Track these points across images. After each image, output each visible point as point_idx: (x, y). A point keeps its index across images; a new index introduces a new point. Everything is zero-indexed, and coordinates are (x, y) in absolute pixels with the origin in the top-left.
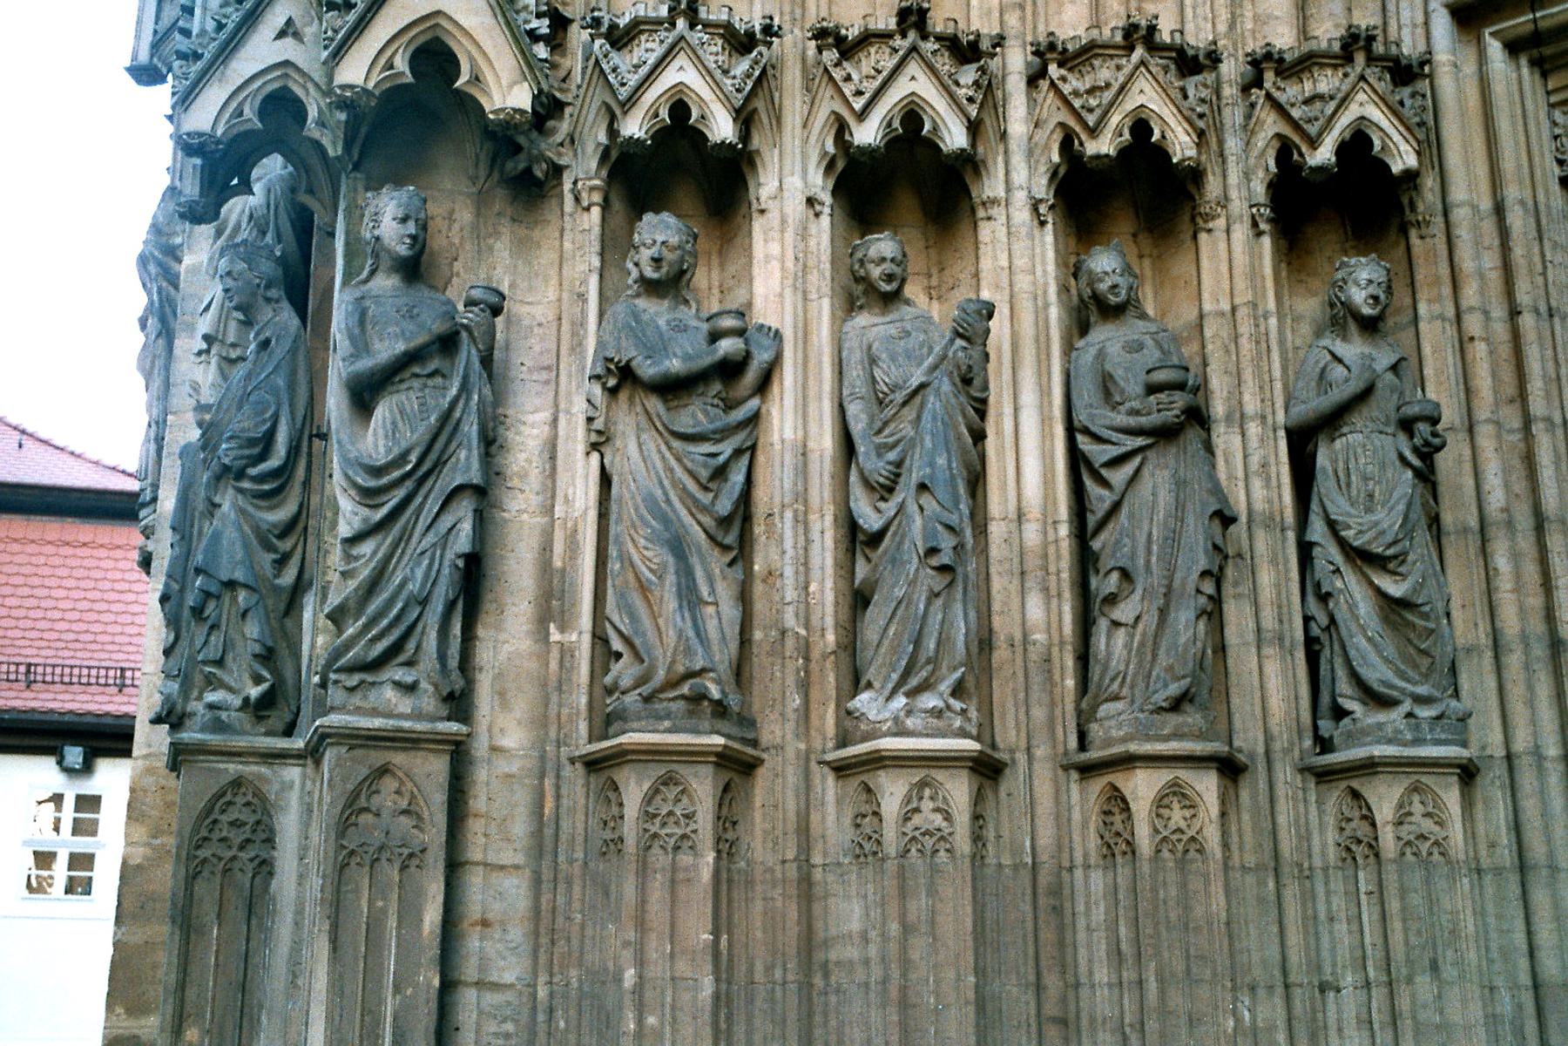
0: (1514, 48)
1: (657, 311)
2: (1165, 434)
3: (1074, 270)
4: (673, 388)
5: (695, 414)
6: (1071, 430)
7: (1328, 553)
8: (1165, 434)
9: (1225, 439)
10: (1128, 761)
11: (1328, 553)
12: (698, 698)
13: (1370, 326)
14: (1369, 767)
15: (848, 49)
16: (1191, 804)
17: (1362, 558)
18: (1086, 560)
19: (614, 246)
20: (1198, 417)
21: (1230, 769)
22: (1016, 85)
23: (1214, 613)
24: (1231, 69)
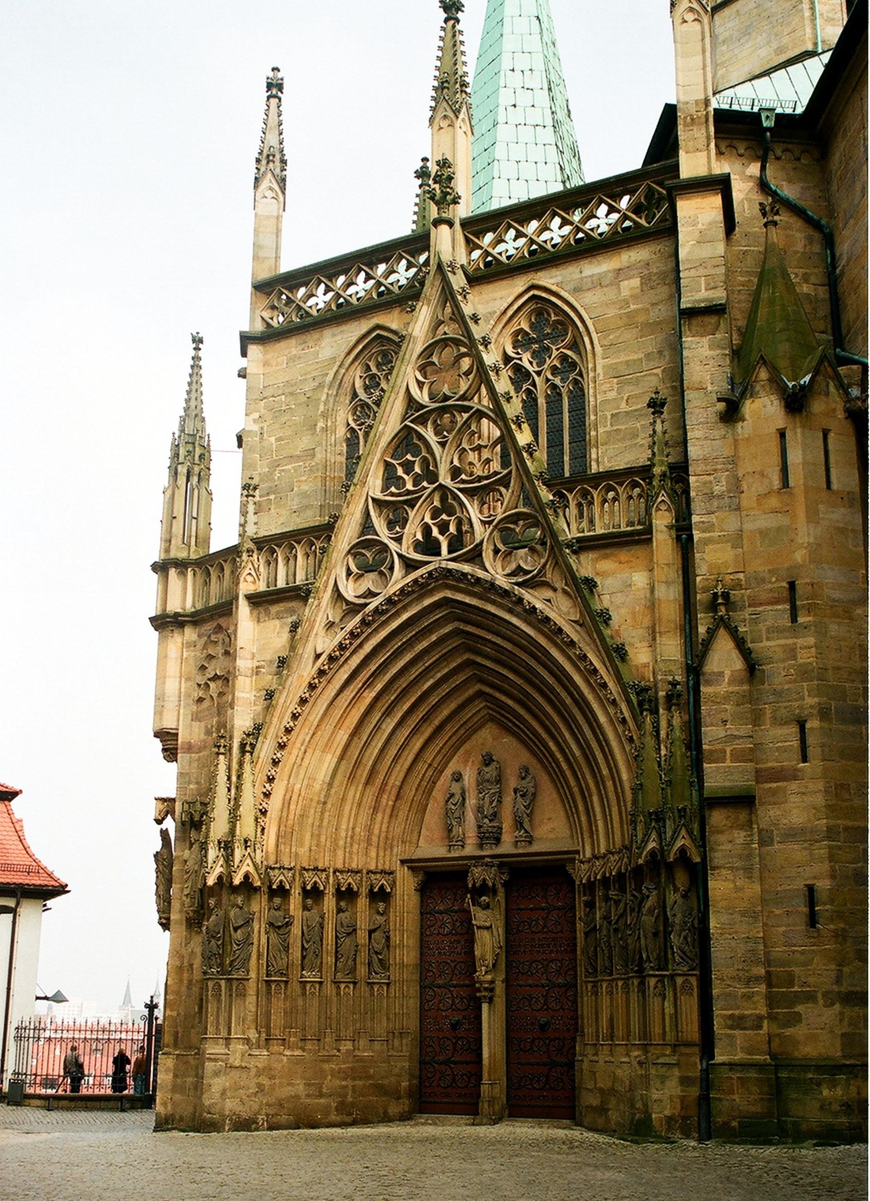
0: (409, 868)
1: (277, 913)
2: (349, 934)
3: (337, 904)
4: (279, 927)
5: (281, 931)
6: (336, 931)
7: (372, 951)
8: (349, 934)
9: (359, 932)
10: (341, 982)
11: (372, 951)
12: (282, 973)
13: (382, 915)
14: (374, 983)
15: (305, 869)
16: (349, 988)
17: (376, 953)
18: (337, 952)
19: (270, 899)
20: (355, 930)
21: (355, 983)
22: (331, 874)
23: (355, 960)
24: (365, 871)
